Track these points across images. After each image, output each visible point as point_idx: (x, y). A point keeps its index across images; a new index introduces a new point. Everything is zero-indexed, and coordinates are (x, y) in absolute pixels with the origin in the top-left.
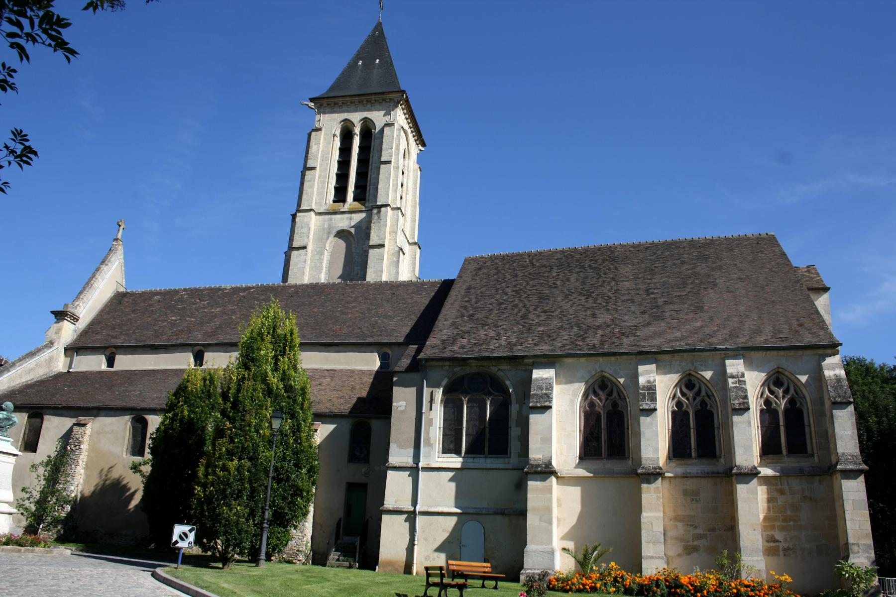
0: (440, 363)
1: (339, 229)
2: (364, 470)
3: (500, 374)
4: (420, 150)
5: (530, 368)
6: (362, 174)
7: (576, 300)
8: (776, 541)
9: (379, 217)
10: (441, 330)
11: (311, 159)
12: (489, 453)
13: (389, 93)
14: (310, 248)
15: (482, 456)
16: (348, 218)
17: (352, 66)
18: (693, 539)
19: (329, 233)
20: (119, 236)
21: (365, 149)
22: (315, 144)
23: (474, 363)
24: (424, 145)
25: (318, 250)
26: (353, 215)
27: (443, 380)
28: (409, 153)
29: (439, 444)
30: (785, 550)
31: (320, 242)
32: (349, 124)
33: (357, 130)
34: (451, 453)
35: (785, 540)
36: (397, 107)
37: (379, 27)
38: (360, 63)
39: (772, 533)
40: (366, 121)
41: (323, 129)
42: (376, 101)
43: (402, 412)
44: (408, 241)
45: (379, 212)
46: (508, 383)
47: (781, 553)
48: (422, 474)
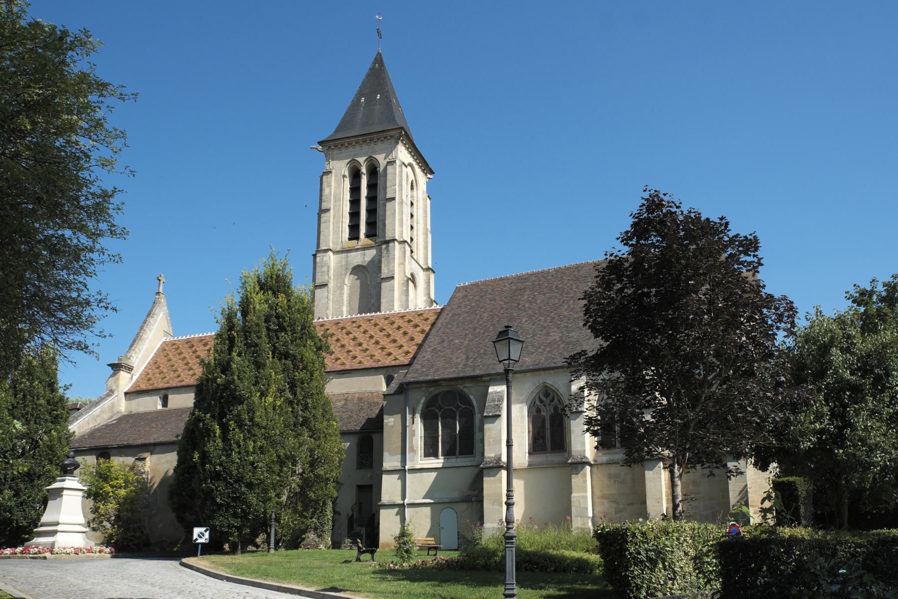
0: (418, 386)
1: (355, 264)
2: (369, 474)
3: (466, 390)
4: (429, 178)
5: (487, 384)
6: (371, 212)
7: (536, 321)
9: (388, 251)
10: (424, 357)
11: (325, 201)
12: (460, 454)
13: (388, 130)
14: (331, 285)
15: (454, 457)
16: (362, 254)
17: (355, 104)
19: (347, 269)
20: (161, 290)
21: (372, 187)
22: (327, 187)
23: (444, 383)
24: (432, 173)
25: (339, 285)
26: (367, 252)
27: (421, 398)
28: (416, 184)
29: (421, 450)
31: (340, 277)
33: (364, 170)
34: (431, 456)
37: (379, 60)
38: (363, 100)
40: (371, 160)
41: (334, 171)
42: (378, 139)
44: (422, 268)
45: (387, 248)
46: (472, 397)
48: (408, 476)
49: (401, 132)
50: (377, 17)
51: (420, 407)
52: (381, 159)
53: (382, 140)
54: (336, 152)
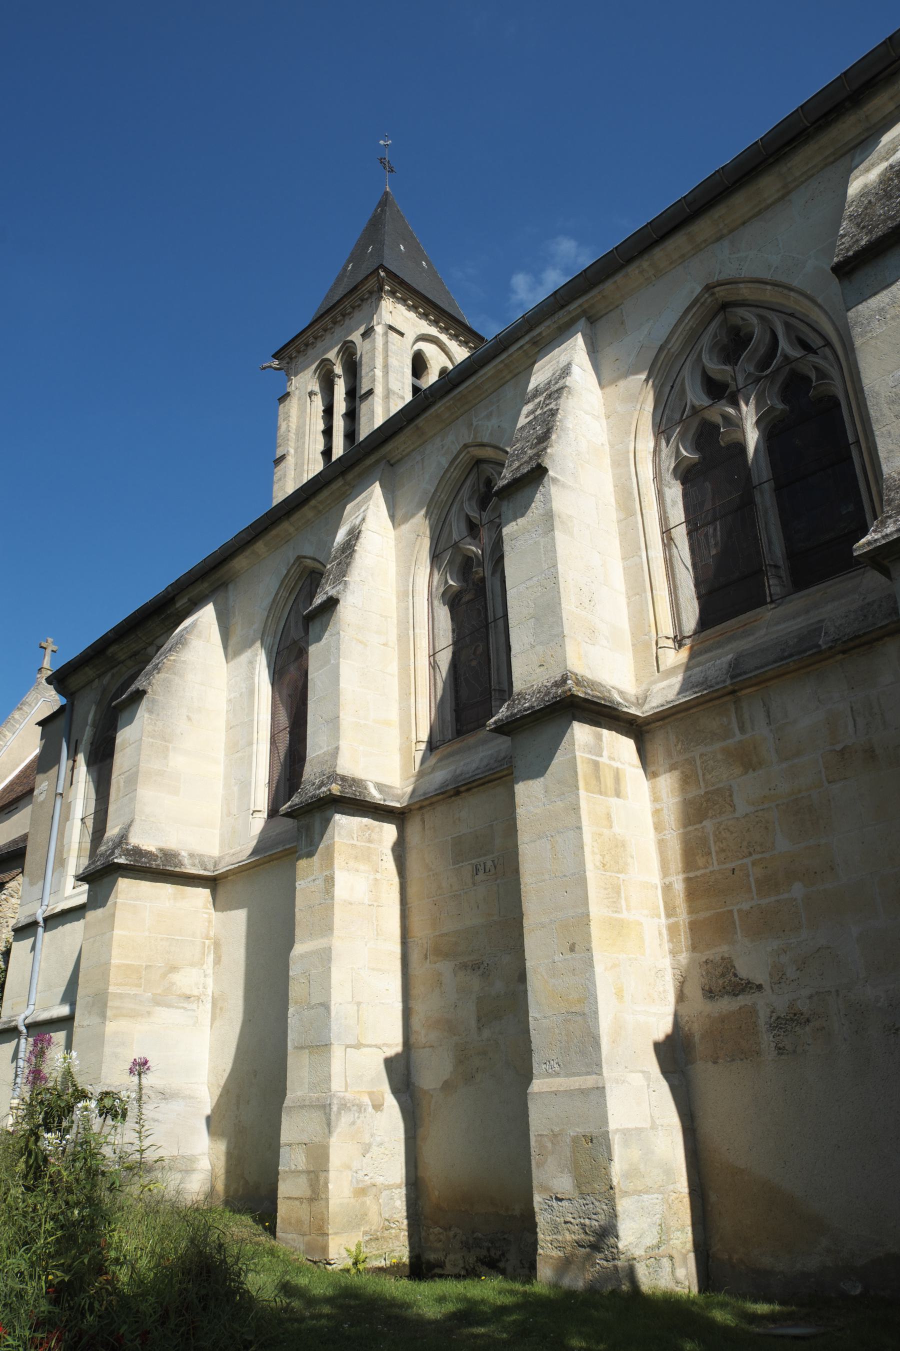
8: (741, 987)
18: (479, 1020)
22: (284, 420)
30: (779, 1024)
32: (329, 367)
33: (338, 370)
35: (779, 977)
36: (380, 298)
37: (384, 202)
39: (724, 949)
43: (43, 802)
47: (767, 1041)
49: (379, 273)
50: (382, 142)
51: (88, 733)
52: (356, 337)
53: (359, 306)
54: (301, 359)
